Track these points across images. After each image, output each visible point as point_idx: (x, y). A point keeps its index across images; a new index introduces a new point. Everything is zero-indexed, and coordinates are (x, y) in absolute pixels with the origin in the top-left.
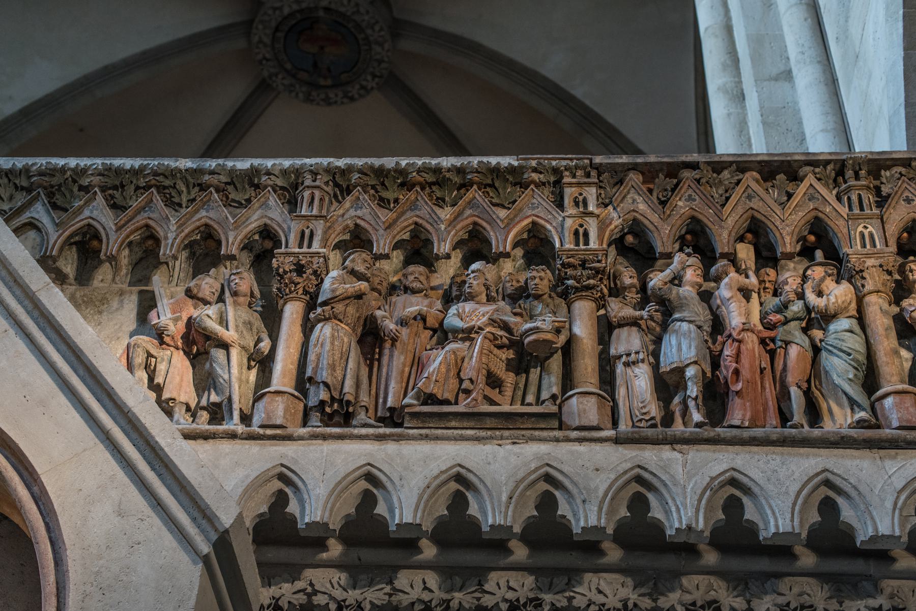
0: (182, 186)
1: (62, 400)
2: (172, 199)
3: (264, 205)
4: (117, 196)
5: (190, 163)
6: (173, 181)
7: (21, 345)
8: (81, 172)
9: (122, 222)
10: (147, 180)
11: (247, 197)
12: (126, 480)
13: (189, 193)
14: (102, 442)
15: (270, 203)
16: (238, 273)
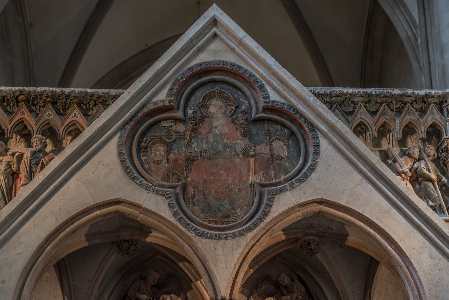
0: (394, 102)
1: (394, 211)
2: (391, 108)
3: (432, 113)
4: (368, 106)
5: (399, 91)
6: (391, 100)
7: (370, 187)
8: (353, 95)
9: (376, 121)
10: (382, 100)
11: (420, 107)
12: (429, 244)
13: (396, 105)
14: (415, 229)
15: (434, 111)
16: (429, 147)
